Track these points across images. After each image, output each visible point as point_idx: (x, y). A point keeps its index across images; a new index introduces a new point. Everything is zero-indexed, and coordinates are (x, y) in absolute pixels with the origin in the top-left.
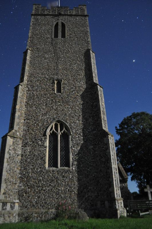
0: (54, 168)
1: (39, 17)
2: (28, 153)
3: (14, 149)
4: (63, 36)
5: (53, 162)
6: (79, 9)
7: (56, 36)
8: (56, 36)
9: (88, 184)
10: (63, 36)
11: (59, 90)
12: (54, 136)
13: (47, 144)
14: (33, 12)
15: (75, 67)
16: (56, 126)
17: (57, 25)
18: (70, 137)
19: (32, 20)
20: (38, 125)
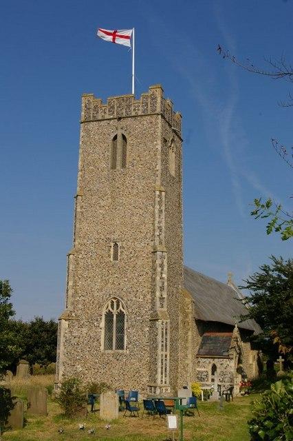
0: (110, 351)
1: (91, 125)
2: (85, 335)
3: (71, 332)
4: (124, 166)
5: (109, 345)
6: (149, 100)
7: (114, 167)
8: (114, 167)
9: (140, 369)
10: (124, 166)
11: (116, 258)
12: (109, 316)
13: (103, 324)
14: (83, 119)
15: (136, 219)
16: (112, 302)
17: (115, 138)
18: (126, 316)
19: (82, 134)
20: (93, 302)
